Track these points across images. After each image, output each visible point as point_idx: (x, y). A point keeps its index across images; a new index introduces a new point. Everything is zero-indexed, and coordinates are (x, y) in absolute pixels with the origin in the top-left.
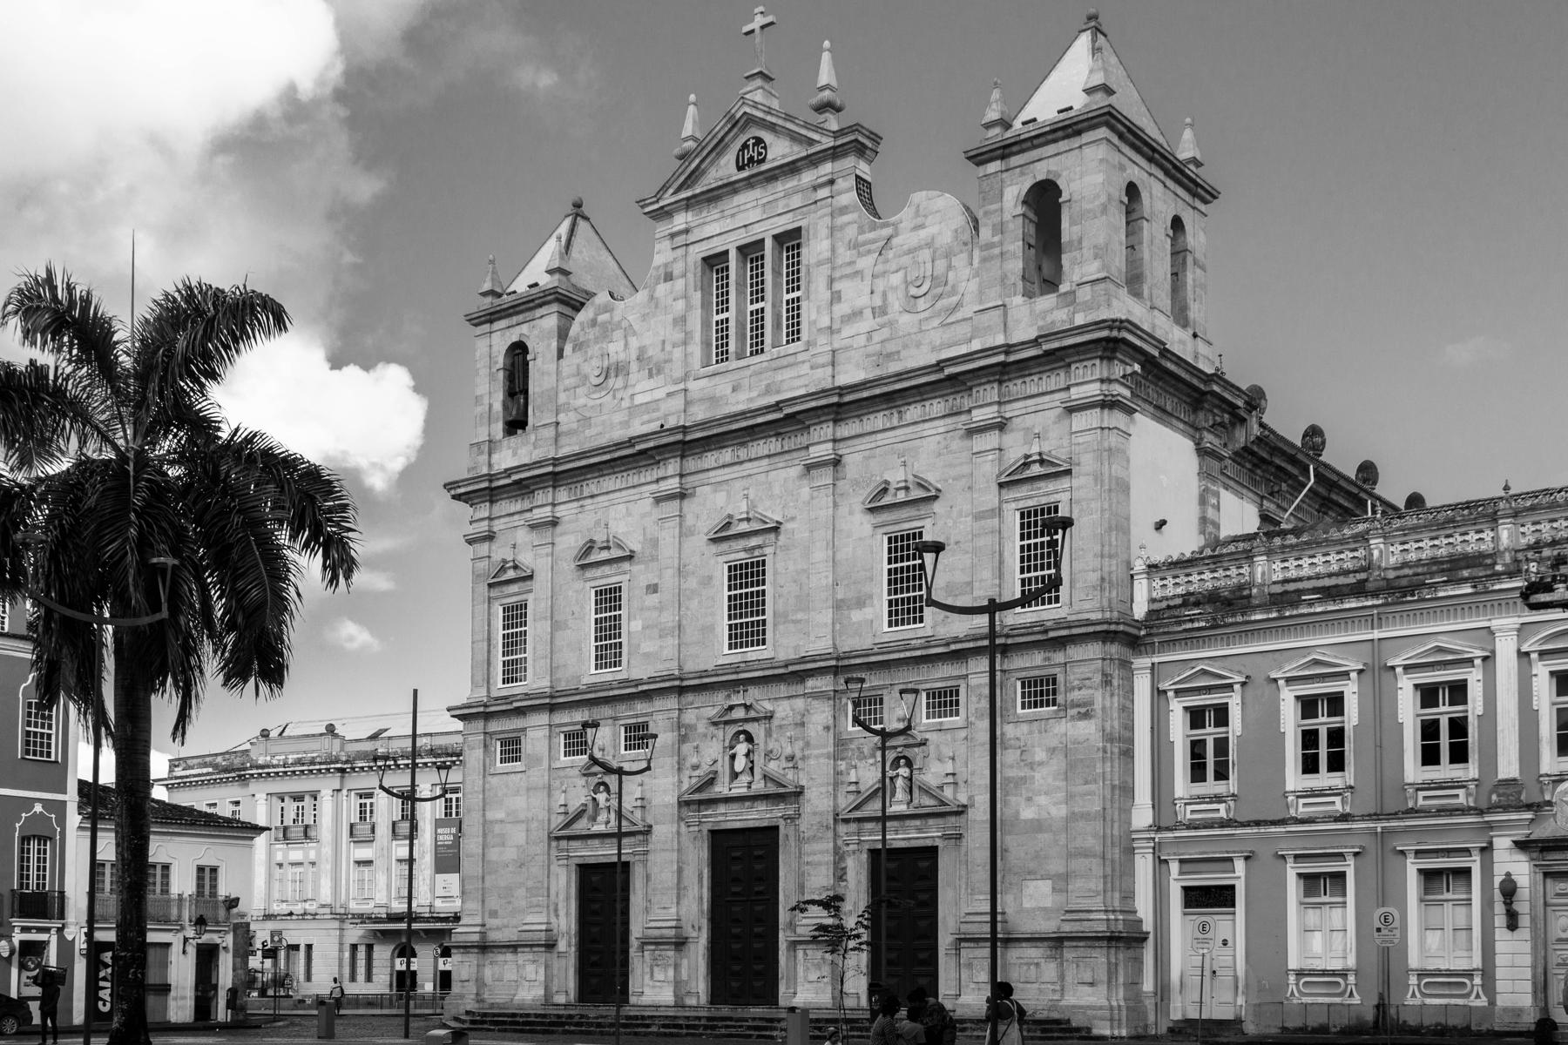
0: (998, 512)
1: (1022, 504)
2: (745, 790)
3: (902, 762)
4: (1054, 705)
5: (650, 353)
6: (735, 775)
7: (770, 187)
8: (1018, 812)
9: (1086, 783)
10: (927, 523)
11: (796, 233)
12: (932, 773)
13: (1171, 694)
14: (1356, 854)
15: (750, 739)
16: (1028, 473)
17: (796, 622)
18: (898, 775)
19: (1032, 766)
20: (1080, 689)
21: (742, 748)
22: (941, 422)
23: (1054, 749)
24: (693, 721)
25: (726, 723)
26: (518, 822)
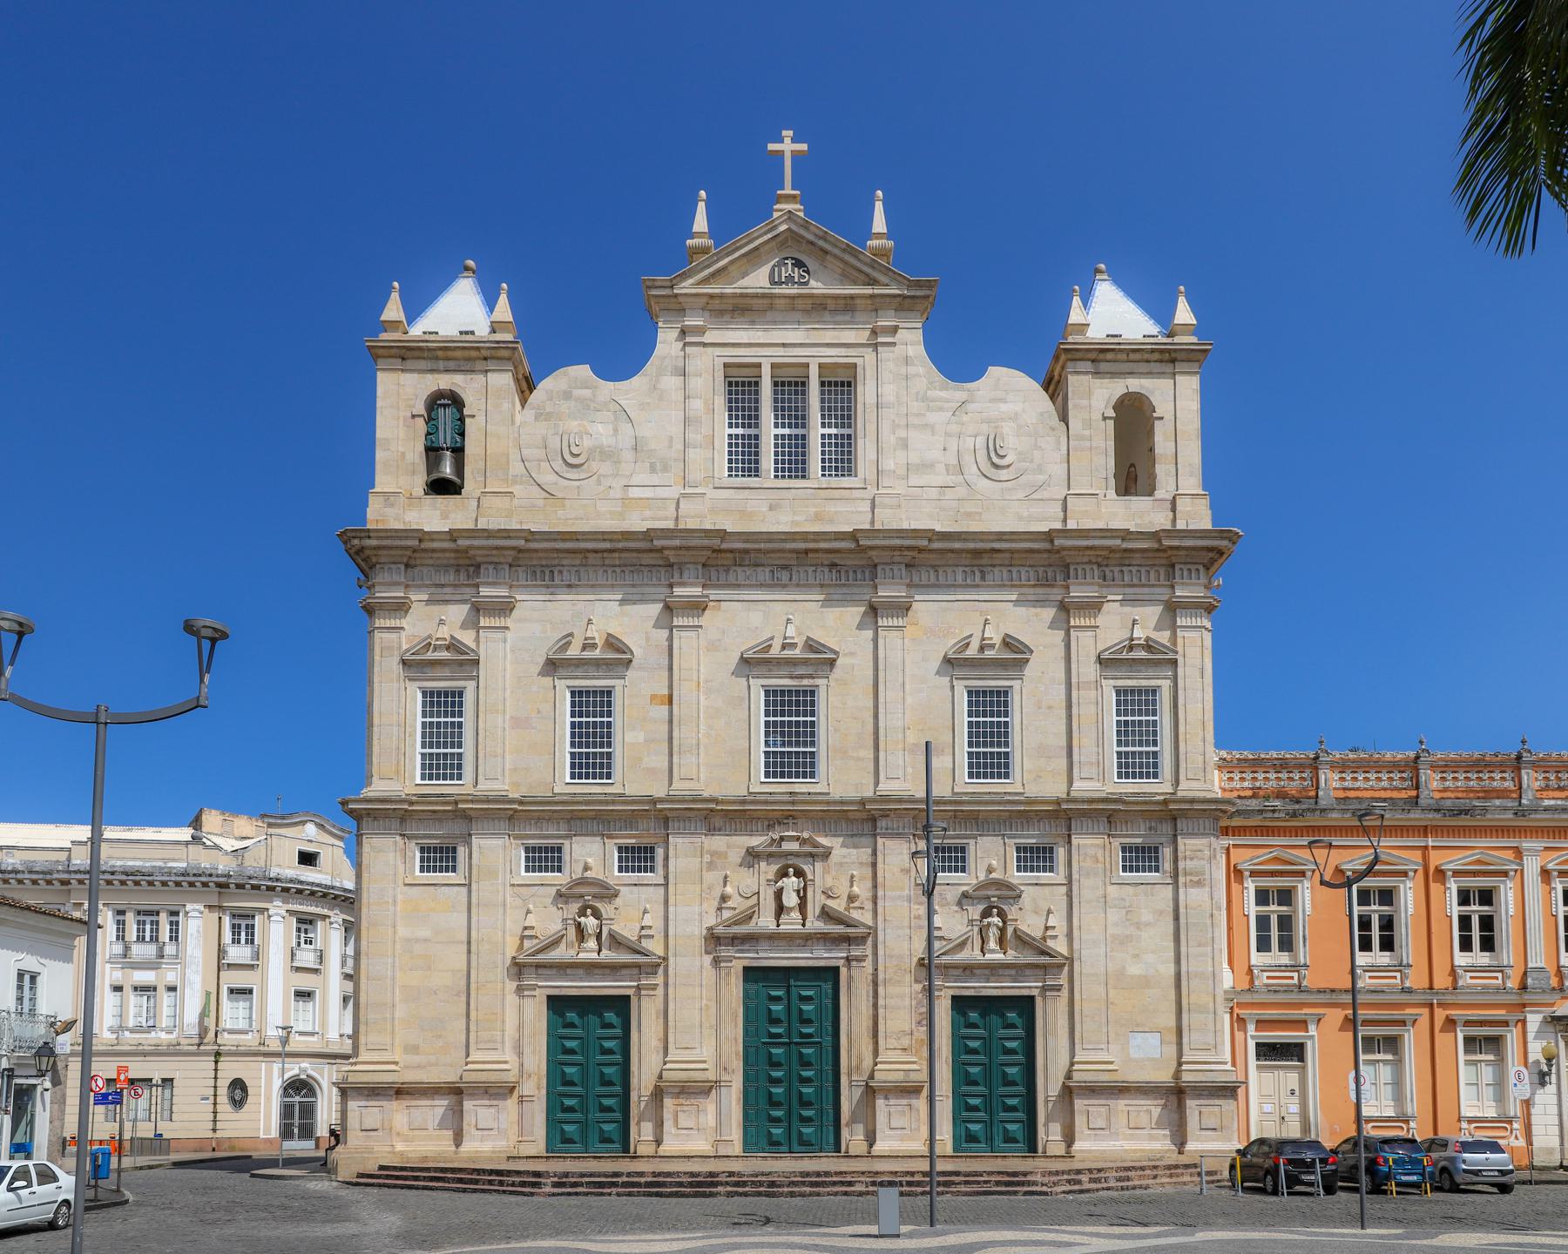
0: (1098, 686)
1: (1120, 683)
4: (1157, 870)
6: (780, 909)
8: (1124, 968)
9: (1199, 945)
10: (1016, 684)
12: (1030, 924)
13: (1247, 873)
16: (1133, 655)
17: (859, 759)
18: (989, 924)
19: (1138, 926)
20: (1192, 859)
21: (791, 882)
22: (1031, 590)
23: (1161, 912)
24: (723, 848)
25: (770, 856)
26: (453, 942)
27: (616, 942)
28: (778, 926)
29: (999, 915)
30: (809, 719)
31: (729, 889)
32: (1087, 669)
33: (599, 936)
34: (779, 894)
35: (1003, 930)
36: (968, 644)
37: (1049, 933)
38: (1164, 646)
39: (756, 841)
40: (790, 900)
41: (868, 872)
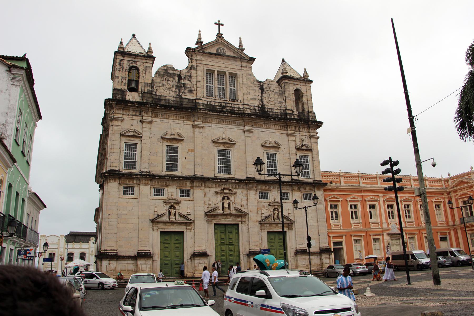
1: (300, 154)
2: (229, 213)
3: (276, 209)
5: (188, 86)
6: (223, 207)
7: (227, 61)
11: (236, 75)
14: (345, 236)
15: (228, 198)
21: (226, 202)
22: (280, 131)
23: (313, 210)
25: (221, 193)
27: (181, 215)
28: (224, 212)
29: (277, 211)
30: (229, 158)
31: (210, 202)
32: (294, 151)
33: (175, 215)
34: (223, 204)
35: (278, 214)
36: (266, 143)
37: (289, 215)
38: (309, 146)
39: (217, 190)
40: (226, 205)
41: (246, 198)
